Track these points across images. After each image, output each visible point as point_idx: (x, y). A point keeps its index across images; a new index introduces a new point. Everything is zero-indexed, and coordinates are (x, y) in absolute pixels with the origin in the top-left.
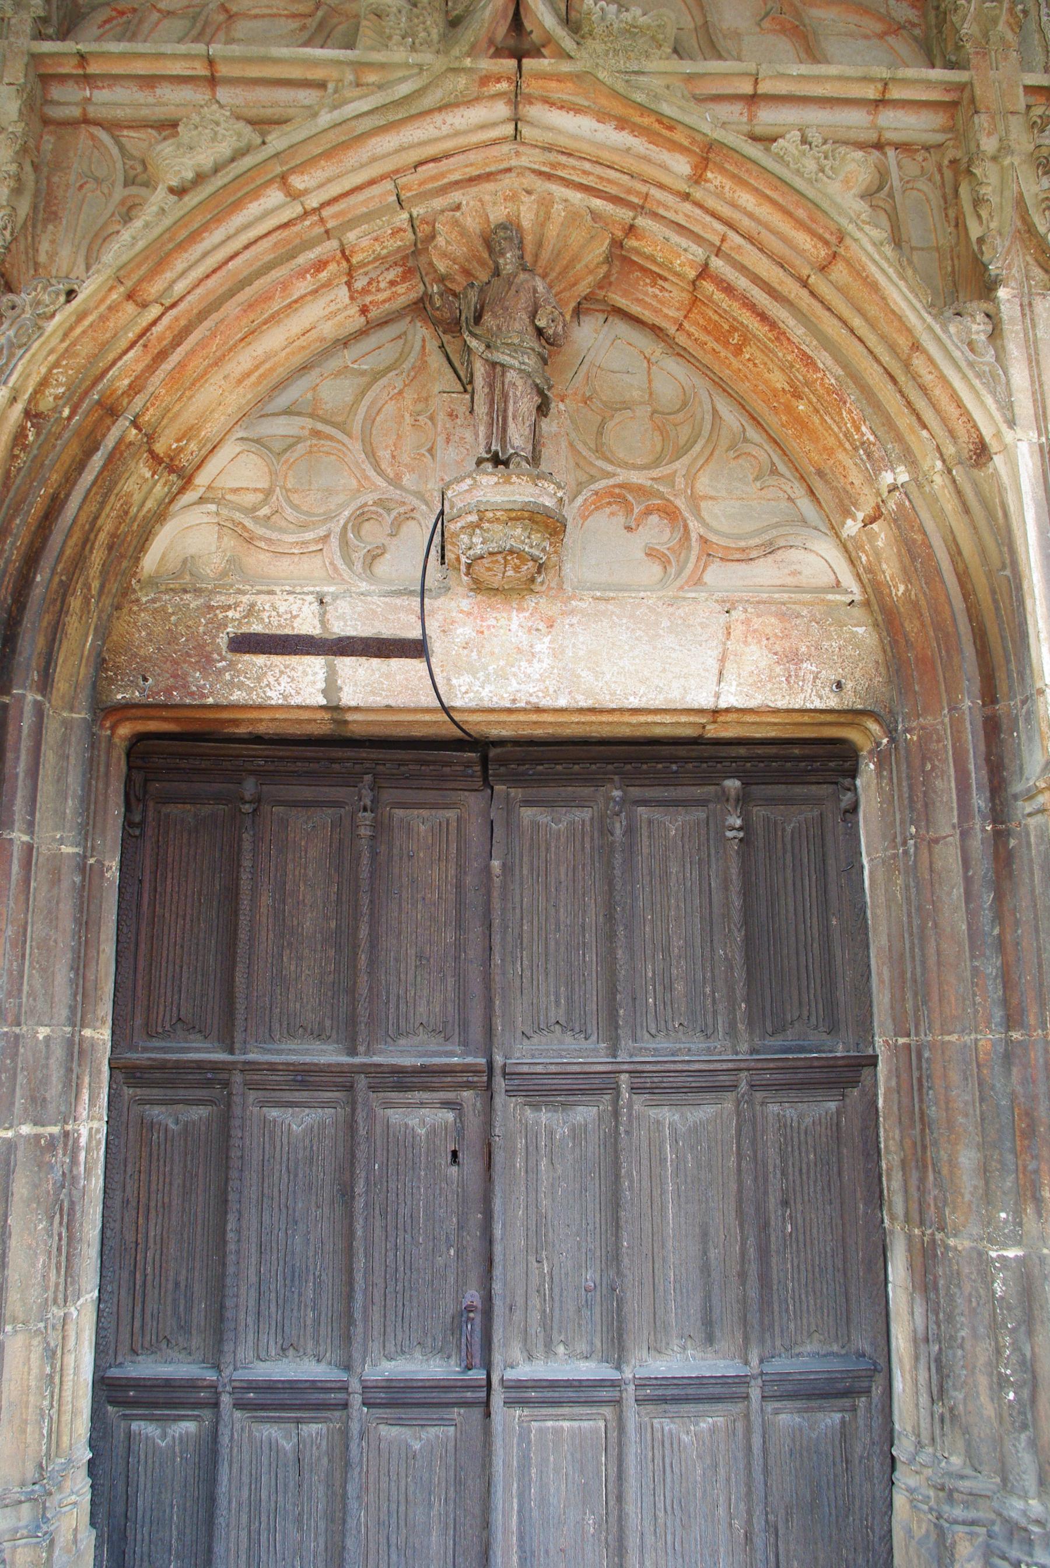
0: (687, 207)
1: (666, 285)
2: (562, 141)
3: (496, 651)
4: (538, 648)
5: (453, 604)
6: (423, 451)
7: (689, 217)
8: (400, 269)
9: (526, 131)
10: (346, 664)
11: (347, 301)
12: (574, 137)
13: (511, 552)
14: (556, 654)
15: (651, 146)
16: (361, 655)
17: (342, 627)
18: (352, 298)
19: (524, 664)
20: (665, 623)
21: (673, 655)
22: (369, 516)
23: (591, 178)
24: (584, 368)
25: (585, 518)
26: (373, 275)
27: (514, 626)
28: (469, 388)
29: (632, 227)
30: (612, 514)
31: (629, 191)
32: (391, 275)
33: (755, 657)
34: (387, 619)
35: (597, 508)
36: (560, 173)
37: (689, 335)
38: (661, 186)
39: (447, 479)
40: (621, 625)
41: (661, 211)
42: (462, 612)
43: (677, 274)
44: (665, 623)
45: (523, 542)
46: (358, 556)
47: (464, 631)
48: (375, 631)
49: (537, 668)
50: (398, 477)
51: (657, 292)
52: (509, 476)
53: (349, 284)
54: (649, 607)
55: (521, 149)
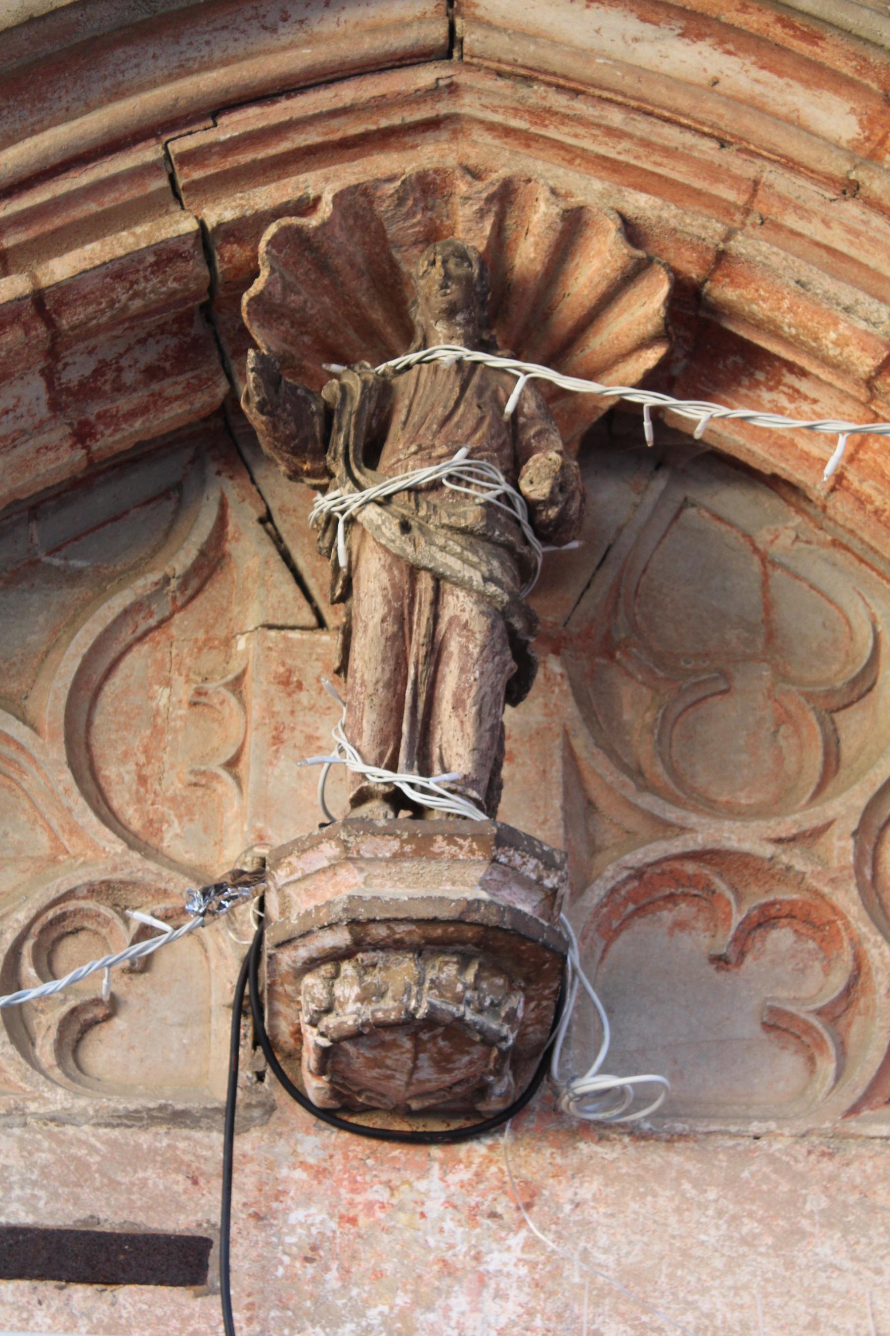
0: (852, 210)
1: (804, 386)
2: (556, 60)
3: (388, 1267)
4: (494, 1261)
5: (282, 1147)
6: (215, 766)
7: (857, 234)
8: (172, 342)
9: (473, 39)
11: (43, 411)
12: (585, 54)
13: (431, 1021)
14: (545, 1279)
15: (765, 75)
16: (42, 1277)
18: (55, 406)
19: (459, 1302)
20: (816, 1201)
21: (838, 1284)
22: (77, 923)
23: (625, 144)
24: (609, 574)
25: (611, 935)
26: (109, 355)
27: (434, 1207)
28: (334, 617)
29: (721, 257)
30: (680, 925)
31: (714, 172)
32: (148, 356)
34: (114, 1184)
35: (640, 911)
36: (552, 133)
37: (861, 501)
38: (791, 165)
39: (278, 839)
40: (703, 1206)
41: (791, 221)
42: (303, 1164)
43: (835, 366)
44: (816, 1201)
45: (459, 999)
47: (306, 1219)
48: (81, 1214)
50: (154, 825)
51: (784, 401)
52: (429, 839)
53: (49, 376)
54: (772, 1159)
55: (464, 78)
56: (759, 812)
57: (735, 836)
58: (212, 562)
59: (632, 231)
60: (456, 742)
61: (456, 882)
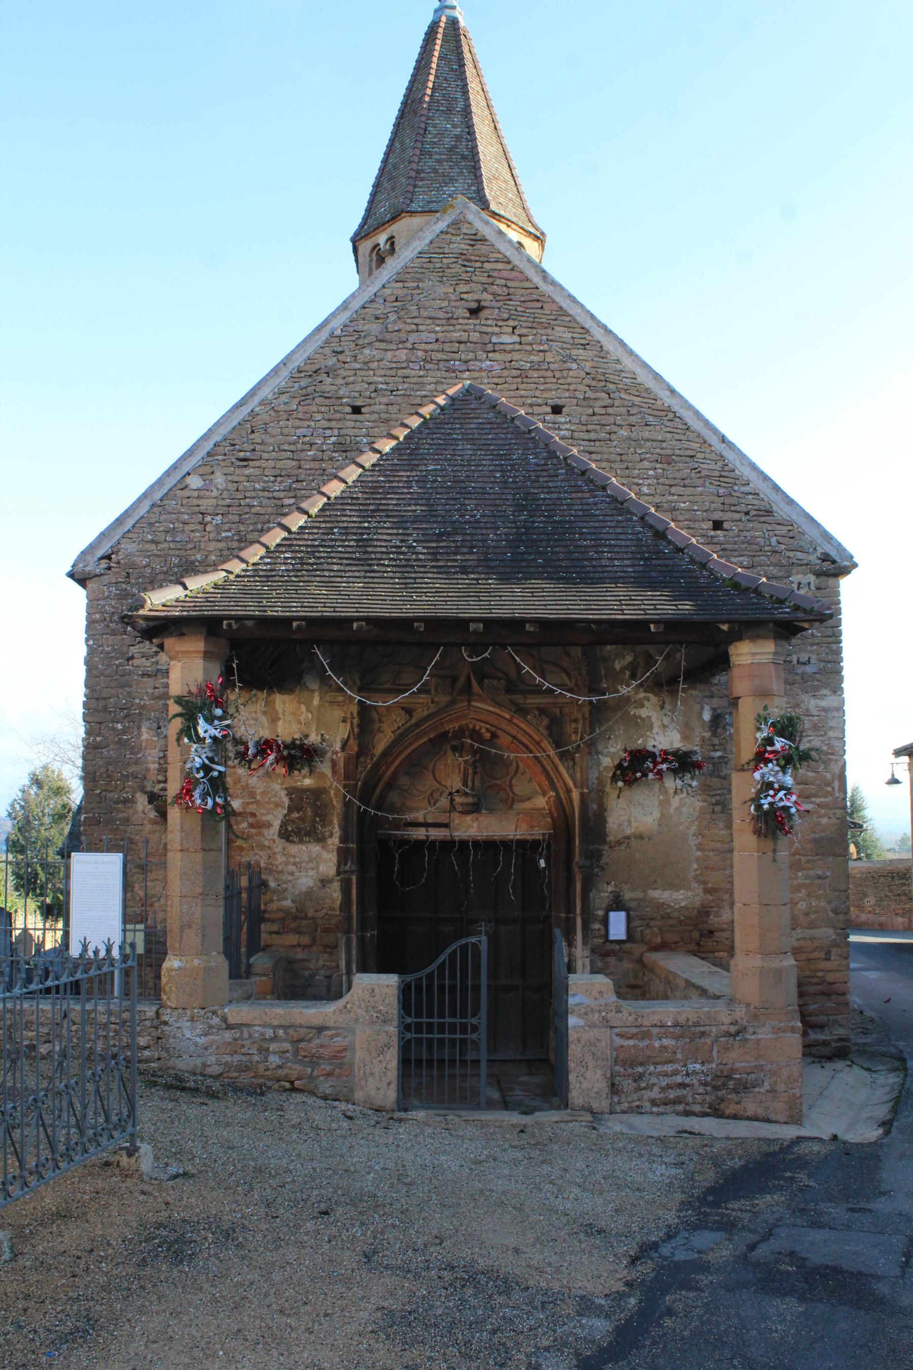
10: (430, 829)
14: (478, 827)
17: (429, 820)
33: (524, 826)
46: (432, 802)
47: (457, 821)
49: (475, 830)
56: (498, 779)
57: (498, 782)
58: (446, 752)
59: (487, 730)
60: (470, 784)
61: (470, 800)
